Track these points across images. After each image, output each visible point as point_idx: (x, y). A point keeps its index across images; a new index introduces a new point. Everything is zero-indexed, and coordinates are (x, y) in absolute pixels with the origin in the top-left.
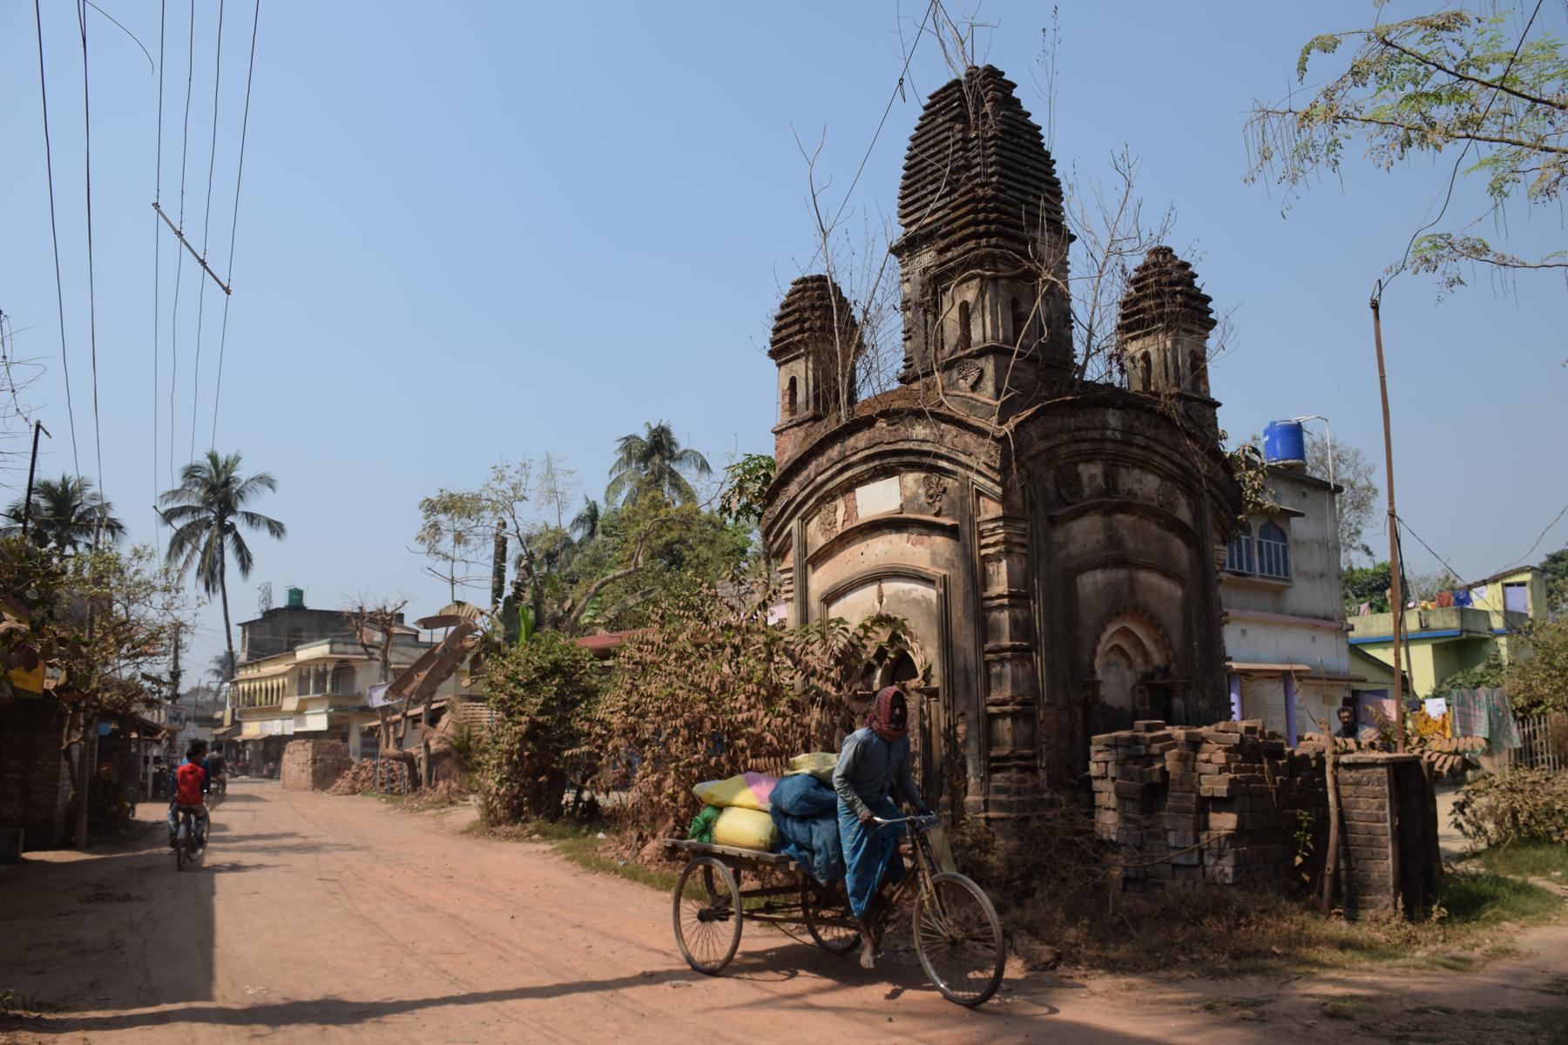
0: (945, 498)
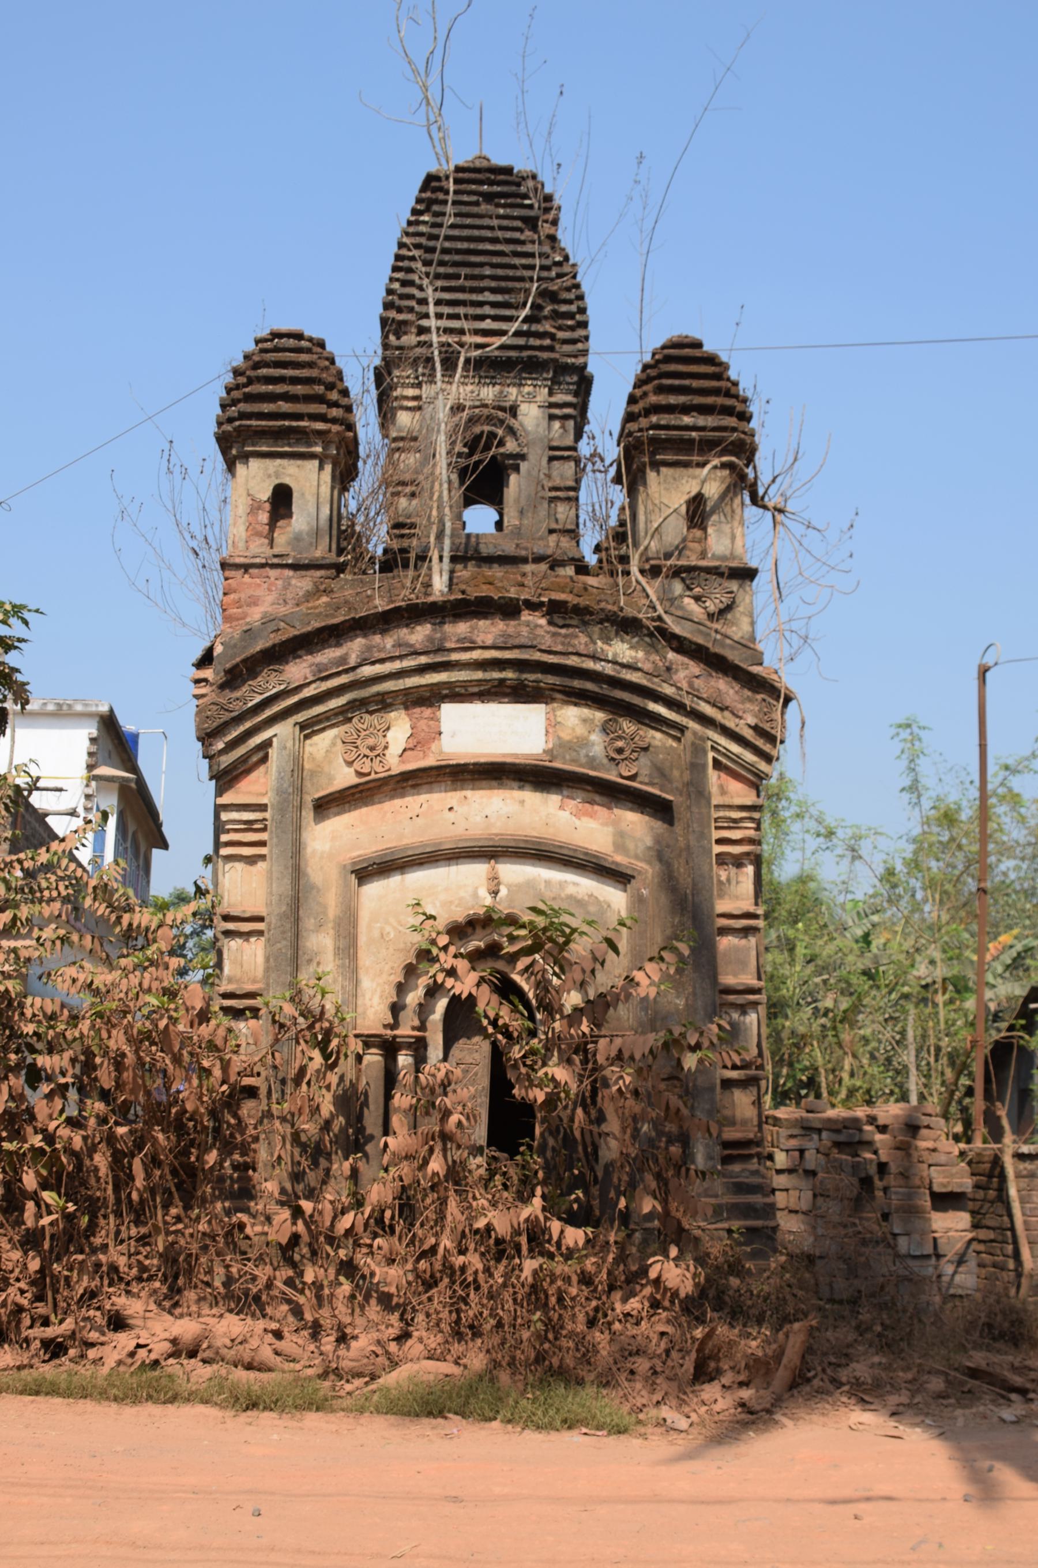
0: (644, 760)
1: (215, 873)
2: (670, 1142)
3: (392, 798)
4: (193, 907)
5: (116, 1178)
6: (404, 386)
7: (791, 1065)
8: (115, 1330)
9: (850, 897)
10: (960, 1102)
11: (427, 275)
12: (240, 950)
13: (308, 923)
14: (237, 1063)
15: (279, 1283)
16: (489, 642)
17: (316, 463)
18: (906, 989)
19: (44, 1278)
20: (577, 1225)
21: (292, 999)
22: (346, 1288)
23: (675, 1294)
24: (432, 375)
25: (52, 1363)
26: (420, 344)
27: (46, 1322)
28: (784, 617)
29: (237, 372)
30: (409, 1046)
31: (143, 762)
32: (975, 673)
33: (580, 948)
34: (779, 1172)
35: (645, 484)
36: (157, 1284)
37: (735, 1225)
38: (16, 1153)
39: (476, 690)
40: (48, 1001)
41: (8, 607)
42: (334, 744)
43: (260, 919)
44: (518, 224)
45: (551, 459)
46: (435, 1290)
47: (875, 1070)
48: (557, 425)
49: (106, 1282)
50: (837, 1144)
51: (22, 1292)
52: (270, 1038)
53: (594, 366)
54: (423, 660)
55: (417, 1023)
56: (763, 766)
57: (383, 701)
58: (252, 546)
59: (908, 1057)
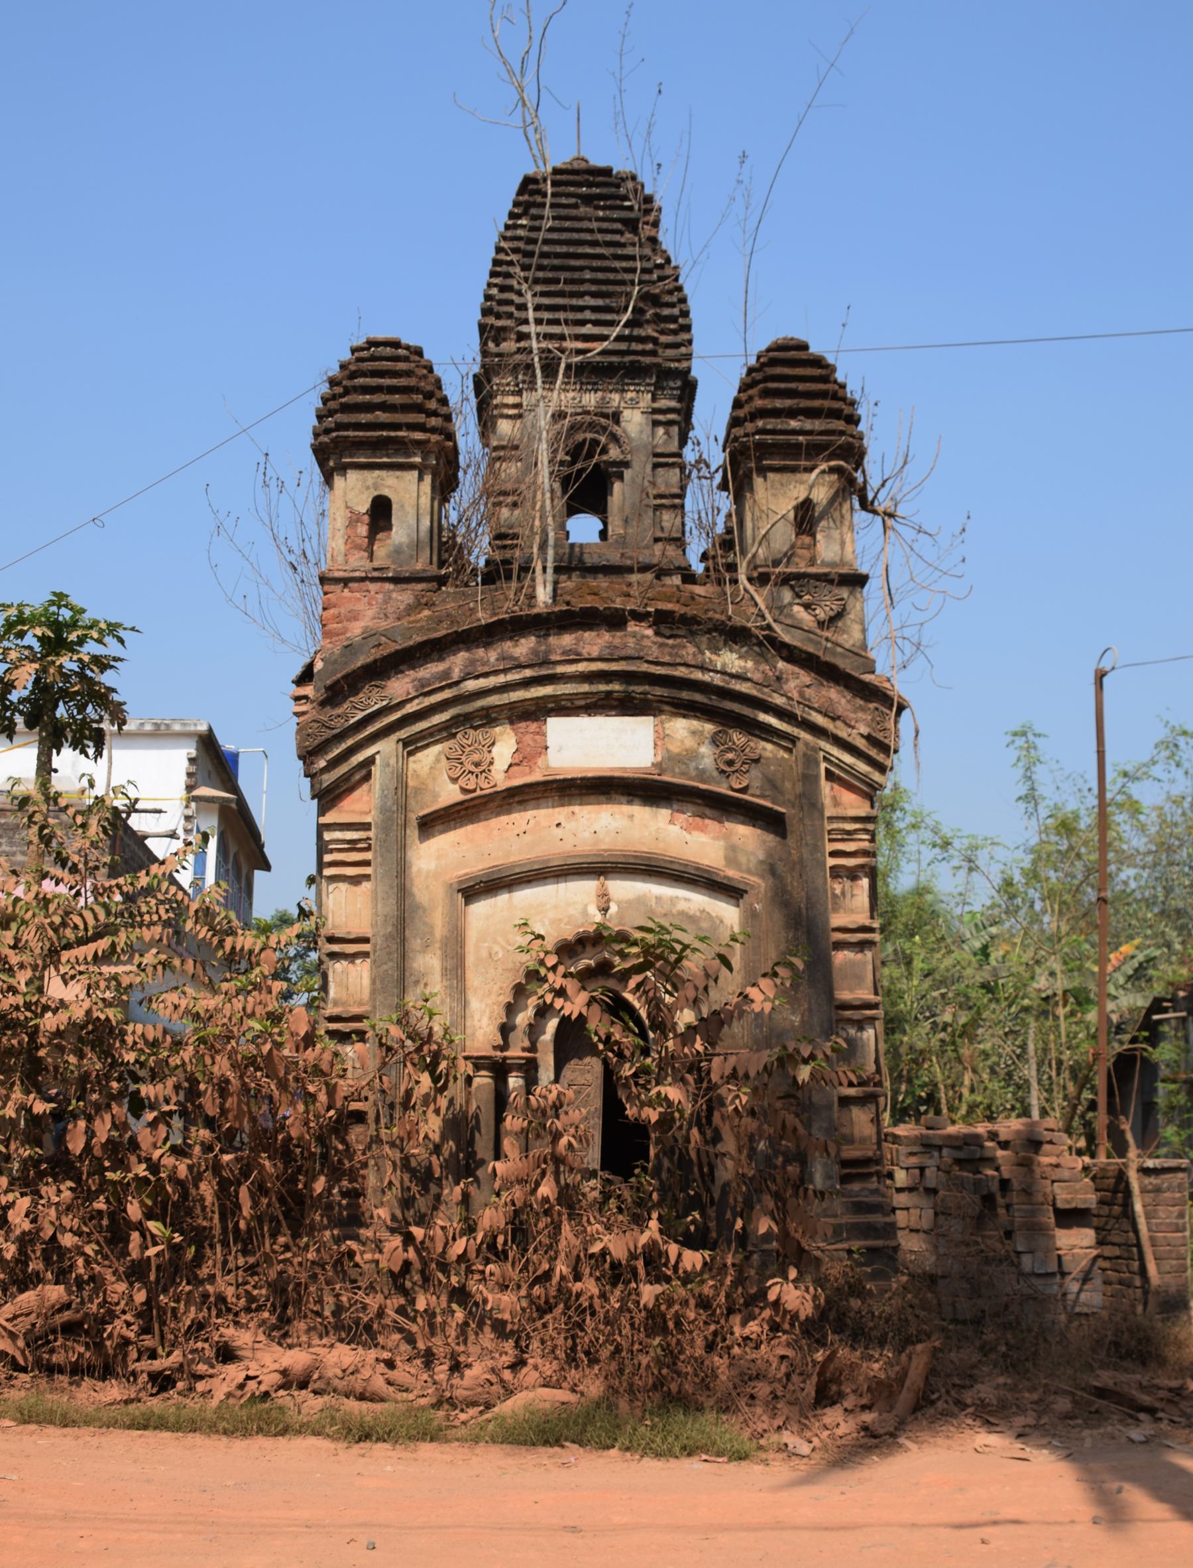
1: (319, 894)
2: (787, 1161)
3: (498, 814)
4: (297, 928)
5: (222, 1208)
6: (504, 393)
7: (910, 1081)
8: (224, 1362)
9: (967, 908)
10: (1082, 1116)
11: (526, 279)
12: (345, 972)
13: (415, 943)
14: (344, 1087)
15: (390, 1312)
16: (595, 654)
17: (416, 473)
18: (1026, 1002)
19: (150, 1309)
20: (695, 1248)
21: (399, 1022)
22: (460, 1315)
23: (795, 1316)
24: (533, 382)
25: (160, 1396)
26: (519, 351)
27: (153, 1355)
28: (896, 624)
29: (333, 382)
30: (519, 1067)
31: (244, 781)
32: (1091, 679)
33: (692, 965)
34: (899, 1190)
35: (752, 490)
36: (266, 1315)
37: (855, 1245)
38: (120, 1182)
39: (582, 703)
40: (150, 1027)
41: (103, 626)
42: (438, 760)
43: (366, 940)
44: (618, 226)
45: (656, 466)
46: (548, 1317)
47: (995, 1085)
48: (661, 431)
49: (214, 1313)
50: (958, 1161)
51: (128, 1324)
52: (378, 1062)
53: (698, 370)
54: (528, 673)
55: (527, 1044)
56: (876, 776)
57: (487, 716)
58: (351, 560)
59: (1029, 1071)
